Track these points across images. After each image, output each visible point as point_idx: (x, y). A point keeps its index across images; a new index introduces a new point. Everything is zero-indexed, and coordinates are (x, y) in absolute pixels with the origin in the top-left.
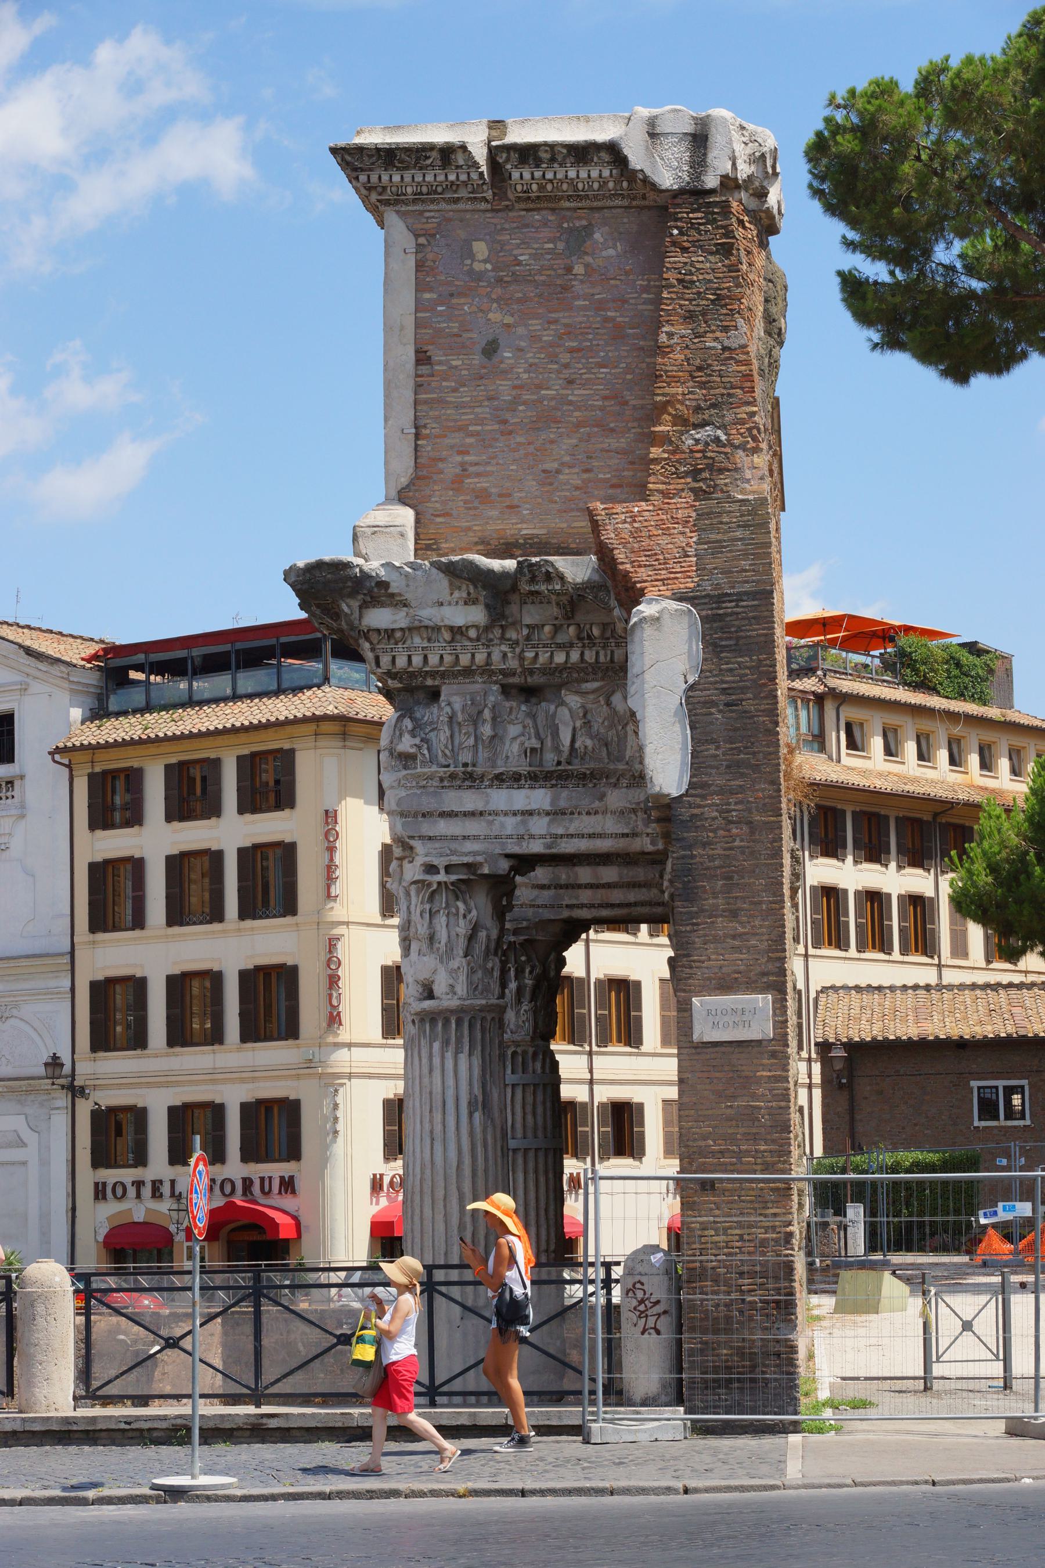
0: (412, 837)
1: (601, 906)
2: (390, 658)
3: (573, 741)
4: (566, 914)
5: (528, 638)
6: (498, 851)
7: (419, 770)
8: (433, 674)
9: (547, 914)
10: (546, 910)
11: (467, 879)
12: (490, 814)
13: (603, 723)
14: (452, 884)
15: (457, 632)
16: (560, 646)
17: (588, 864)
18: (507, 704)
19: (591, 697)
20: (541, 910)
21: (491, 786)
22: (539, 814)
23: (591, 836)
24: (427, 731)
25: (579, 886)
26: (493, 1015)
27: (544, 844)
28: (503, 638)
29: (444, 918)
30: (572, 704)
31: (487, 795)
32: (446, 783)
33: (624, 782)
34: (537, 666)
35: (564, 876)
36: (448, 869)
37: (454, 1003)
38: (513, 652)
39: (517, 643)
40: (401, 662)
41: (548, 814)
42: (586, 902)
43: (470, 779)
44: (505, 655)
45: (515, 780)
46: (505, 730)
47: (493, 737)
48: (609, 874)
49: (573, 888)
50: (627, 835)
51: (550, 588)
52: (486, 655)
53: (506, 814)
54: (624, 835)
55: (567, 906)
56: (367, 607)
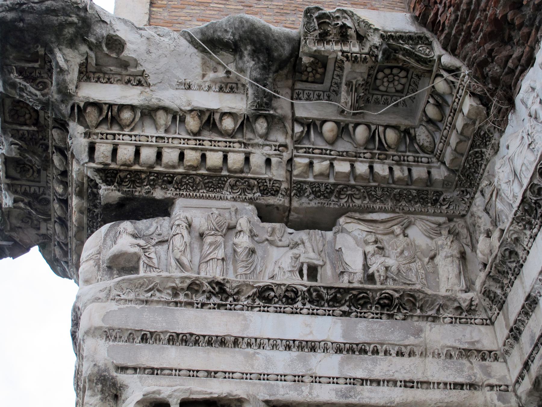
0: (123, 369)
2: (110, 148)
5: (299, 141)
8: (168, 180)
12: (249, 345)
13: (402, 252)
15: (209, 120)
16: (343, 155)
19: (381, 227)
22: (325, 350)
23: (408, 384)
31: (245, 319)
32: (181, 298)
33: (447, 314)
34: (311, 179)
39: (285, 146)
40: (126, 153)
41: (339, 350)
44: (268, 162)
47: (252, 252)
51: (345, 49)
52: (242, 156)
53: (274, 346)
56: (88, 79)
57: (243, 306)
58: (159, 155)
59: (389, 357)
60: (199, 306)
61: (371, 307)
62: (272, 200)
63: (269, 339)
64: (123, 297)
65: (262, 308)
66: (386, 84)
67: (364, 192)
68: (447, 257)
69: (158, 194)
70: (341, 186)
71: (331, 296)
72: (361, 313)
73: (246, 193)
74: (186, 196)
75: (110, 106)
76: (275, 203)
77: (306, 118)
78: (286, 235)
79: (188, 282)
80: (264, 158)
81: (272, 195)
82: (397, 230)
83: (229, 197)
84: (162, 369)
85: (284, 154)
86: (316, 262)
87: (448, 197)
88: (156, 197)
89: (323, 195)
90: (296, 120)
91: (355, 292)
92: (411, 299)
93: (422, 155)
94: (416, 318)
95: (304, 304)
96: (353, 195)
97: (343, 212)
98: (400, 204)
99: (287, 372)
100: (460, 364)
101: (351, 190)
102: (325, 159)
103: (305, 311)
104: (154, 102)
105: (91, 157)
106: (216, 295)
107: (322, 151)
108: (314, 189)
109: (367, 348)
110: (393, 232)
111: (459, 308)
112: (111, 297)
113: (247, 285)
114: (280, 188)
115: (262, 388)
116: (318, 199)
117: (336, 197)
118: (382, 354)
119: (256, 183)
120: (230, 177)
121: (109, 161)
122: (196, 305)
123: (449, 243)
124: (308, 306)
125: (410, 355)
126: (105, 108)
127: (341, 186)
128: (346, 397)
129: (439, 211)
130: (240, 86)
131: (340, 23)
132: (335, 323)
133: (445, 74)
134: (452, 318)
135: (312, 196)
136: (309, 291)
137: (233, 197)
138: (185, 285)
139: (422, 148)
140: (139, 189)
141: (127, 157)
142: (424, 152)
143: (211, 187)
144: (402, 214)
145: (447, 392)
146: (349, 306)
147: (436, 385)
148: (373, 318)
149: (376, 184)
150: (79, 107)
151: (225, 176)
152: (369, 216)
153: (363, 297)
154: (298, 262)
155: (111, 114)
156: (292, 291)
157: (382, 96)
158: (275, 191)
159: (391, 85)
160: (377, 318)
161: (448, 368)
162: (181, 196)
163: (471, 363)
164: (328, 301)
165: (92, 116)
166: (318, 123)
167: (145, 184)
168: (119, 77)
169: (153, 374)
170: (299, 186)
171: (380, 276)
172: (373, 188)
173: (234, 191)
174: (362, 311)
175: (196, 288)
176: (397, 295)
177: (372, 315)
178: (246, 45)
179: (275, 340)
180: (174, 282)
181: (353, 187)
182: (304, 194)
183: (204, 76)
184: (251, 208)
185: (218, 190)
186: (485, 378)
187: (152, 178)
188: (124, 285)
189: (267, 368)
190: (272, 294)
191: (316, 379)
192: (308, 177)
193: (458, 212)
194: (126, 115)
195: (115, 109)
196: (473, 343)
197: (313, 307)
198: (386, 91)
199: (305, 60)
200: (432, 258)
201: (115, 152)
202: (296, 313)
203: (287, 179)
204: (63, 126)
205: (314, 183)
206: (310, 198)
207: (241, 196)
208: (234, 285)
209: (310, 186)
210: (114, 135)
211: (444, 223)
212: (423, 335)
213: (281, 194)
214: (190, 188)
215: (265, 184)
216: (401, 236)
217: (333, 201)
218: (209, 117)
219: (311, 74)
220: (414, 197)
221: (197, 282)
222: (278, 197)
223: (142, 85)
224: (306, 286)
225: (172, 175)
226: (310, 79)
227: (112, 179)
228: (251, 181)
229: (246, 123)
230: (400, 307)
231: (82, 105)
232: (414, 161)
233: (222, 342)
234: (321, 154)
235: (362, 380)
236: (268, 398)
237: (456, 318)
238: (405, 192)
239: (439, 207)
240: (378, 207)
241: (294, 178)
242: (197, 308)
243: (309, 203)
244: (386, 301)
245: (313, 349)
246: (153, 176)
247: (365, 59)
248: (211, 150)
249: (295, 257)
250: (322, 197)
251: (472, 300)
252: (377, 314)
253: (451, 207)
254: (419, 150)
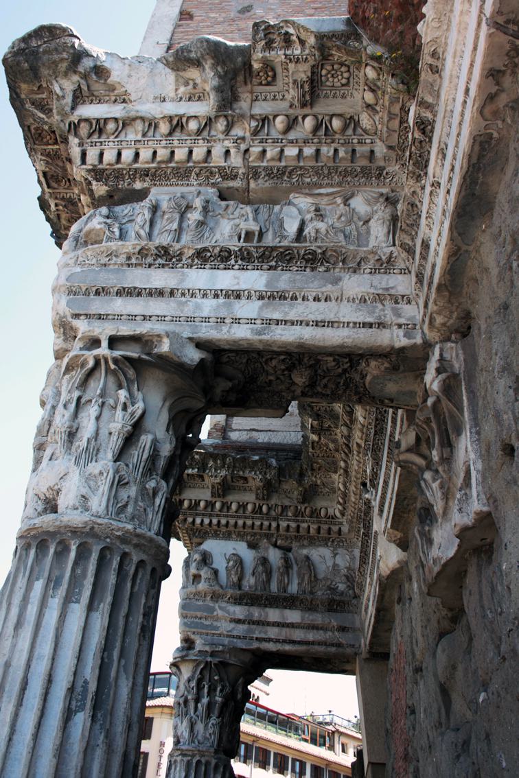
0: (77, 316)
1: (284, 641)
2: (98, 152)
3: (301, 230)
4: (255, 645)
5: (256, 133)
6: (187, 334)
8: (145, 173)
9: (241, 644)
10: (239, 641)
11: (135, 361)
12: (183, 295)
14: (115, 361)
15: (177, 124)
17: (277, 607)
18: (224, 203)
19: (326, 199)
20: (235, 640)
22: (249, 297)
25: (268, 624)
26: (144, 557)
27: (252, 330)
28: (227, 131)
29: (96, 407)
31: (183, 274)
33: (367, 267)
34: (265, 164)
35: (257, 614)
36: (114, 342)
37: (77, 519)
38: (238, 148)
39: (243, 139)
40: (110, 156)
41: (261, 298)
42: (272, 637)
43: (167, 258)
44: (227, 152)
45: (224, 258)
46: (217, 223)
48: (294, 616)
49: (263, 624)
50: (371, 325)
51: (289, 52)
53: (205, 296)
54: (364, 325)
55: (257, 639)
58: (137, 155)
59: (306, 302)
61: (296, 262)
62: (231, 184)
63: (200, 290)
66: (331, 79)
68: (378, 219)
69: (138, 185)
75: (98, 120)
77: (260, 115)
78: (238, 210)
80: (224, 150)
81: (232, 179)
82: (339, 200)
83: (195, 183)
84: (107, 315)
85: (242, 145)
90: (252, 117)
91: (281, 250)
93: (366, 136)
95: (236, 262)
99: (212, 315)
100: (373, 307)
102: (277, 147)
103: (237, 267)
104: (133, 114)
105: (84, 161)
107: (275, 141)
109: (287, 295)
115: (187, 328)
117: (288, 177)
118: (300, 300)
121: (97, 163)
123: (383, 208)
124: (240, 262)
125: (326, 300)
126: (94, 122)
128: (260, 335)
130: (206, 94)
131: (283, 32)
132: (261, 275)
133: (372, 63)
135: (267, 178)
138: (137, 250)
139: (365, 131)
141: (110, 158)
142: (368, 134)
145: (355, 330)
147: (346, 325)
150: (74, 123)
153: (289, 253)
155: (99, 127)
157: (331, 91)
159: (336, 80)
161: (360, 310)
162: (155, 185)
163: (383, 305)
165: (84, 130)
166: (271, 117)
168: (108, 98)
169: (100, 318)
178: (206, 60)
179: (205, 290)
183: (176, 90)
186: (394, 318)
189: (194, 312)
190: (209, 254)
191: (237, 321)
194: (111, 126)
195: (102, 122)
196: (387, 289)
198: (333, 86)
199: (256, 66)
200: (366, 222)
201: (101, 155)
204: (65, 141)
208: (176, 248)
210: (101, 142)
212: (341, 283)
216: (342, 205)
218: (178, 121)
219: (263, 78)
223: (126, 103)
226: (263, 82)
229: (209, 122)
231: (76, 122)
232: (358, 143)
233: (160, 293)
234: (273, 142)
235: (278, 321)
236: (191, 335)
244: (310, 257)
245: (238, 297)
247: (306, 59)
248: (179, 147)
252: (301, 267)
254: (363, 133)
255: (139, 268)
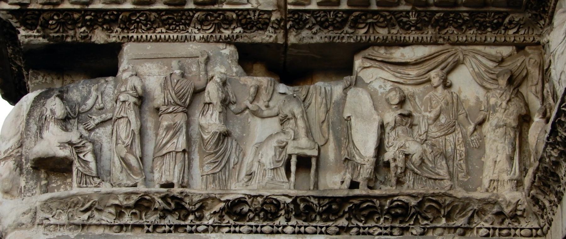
3: (380, 149)
7: (75, 190)
13: (437, 118)
18: (251, 82)
19: (413, 72)
21: (217, 228)
24: (92, 124)
30: (376, 85)
32: (127, 219)
46: (245, 128)
47: (225, 135)
57: (208, 226)
60: (150, 229)
61: (379, 219)
64: (53, 221)
65: (232, 229)
67: (391, 18)
68: (498, 126)
69: (99, 37)
70: (357, 13)
71: (324, 208)
72: (364, 228)
73: (222, 30)
74: (138, 40)
76: (264, 41)
79: (135, 198)
82: (435, 76)
83: (198, 37)
86: (309, 153)
87: (517, 20)
88: (96, 42)
89: (332, 24)
91: (356, 202)
92: (434, 204)
94: (439, 231)
95: (288, 220)
96: (375, 23)
97: (360, 47)
98: (445, 31)
101: (372, 18)
103: (289, 229)
106: (171, 212)
108: (319, 19)
110: (429, 81)
111: (500, 214)
112: (38, 221)
113: (214, 199)
114: (269, 19)
116: (326, 31)
117: (351, 27)
119: (234, 16)
120: (197, 10)
122: (146, 228)
123: (504, 104)
124: (293, 222)
127: (357, 13)
129: (503, 39)
134: (489, 229)
136: (294, 202)
137: (203, 37)
138: (131, 202)
140: (71, 33)
143: (172, 24)
144: (447, 46)
146: (348, 219)
148: (380, 234)
149: (409, 8)
151: (191, 10)
152: (399, 54)
154: (284, 153)
156: (271, 203)
158: (263, 25)
160: (386, 234)
162: (130, 39)
164: (320, 214)
167: (80, 25)
170: (296, 16)
171: (396, 167)
172: (404, 13)
173: (205, 28)
174: (366, 225)
175: (146, 204)
176: (413, 202)
177: (379, 231)
180: (117, 198)
181: (375, 13)
182: (305, 25)
184: (228, 50)
185: (181, 27)
187: (88, 17)
188: (54, 205)
192: (309, 4)
193: (532, 39)
197: (300, 222)
200: (481, 124)
202: (278, 233)
203: (279, 6)
205: (319, 11)
206: (314, 30)
207: (214, 35)
208: (196, 199)
209: (312, 15)
211: (510, 55)
213: (272, 27)
214: (143, 27)
215: (248, 16)
216: (440, 88)
217: (347, 33)
220: (465, 22)
221: (147, 197)
222: (267, 33)
224: (290, 197)
225: (115, 13)
227: (34, 21)
228: (228, 14)
230: (419, 217)
237: (494, 229)
238: (452, 15)
239: (503, 32)
240: (412, 39)
241: (289, 7)
242: (148, 232)
243: (312, 38)
244: (399, 211)
246: (90, 15)
249: (280, 147)
250: (330, 29)
251: (517, 204)
253: (522, 32)
255: (138, 231)
